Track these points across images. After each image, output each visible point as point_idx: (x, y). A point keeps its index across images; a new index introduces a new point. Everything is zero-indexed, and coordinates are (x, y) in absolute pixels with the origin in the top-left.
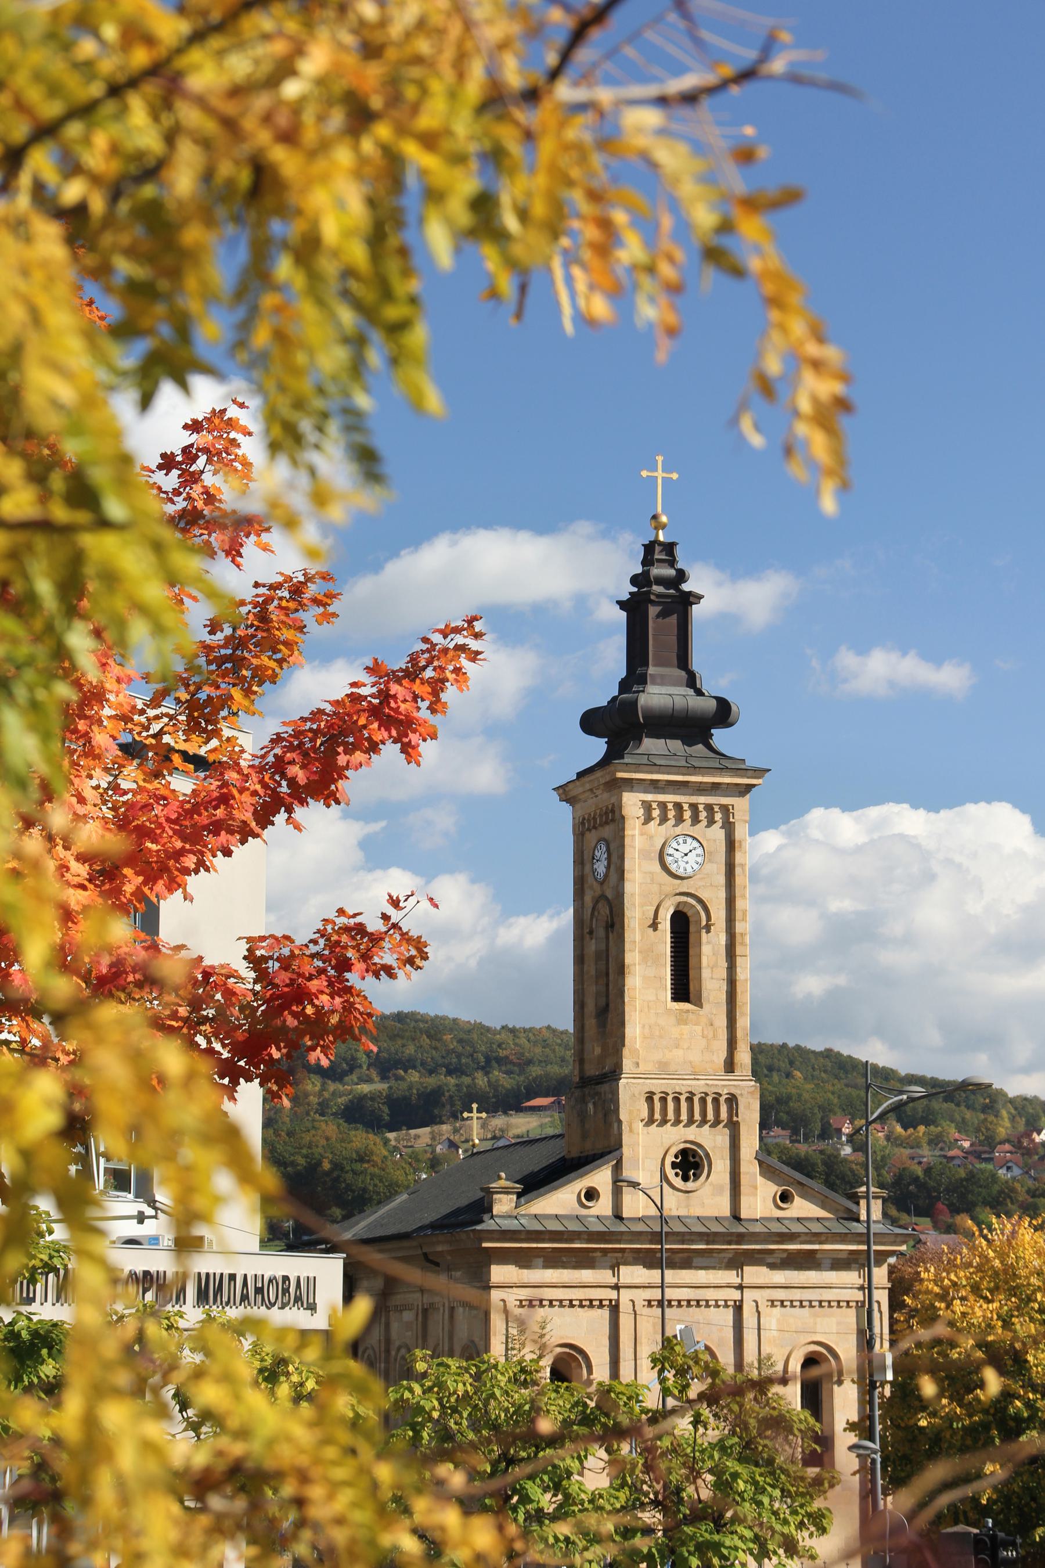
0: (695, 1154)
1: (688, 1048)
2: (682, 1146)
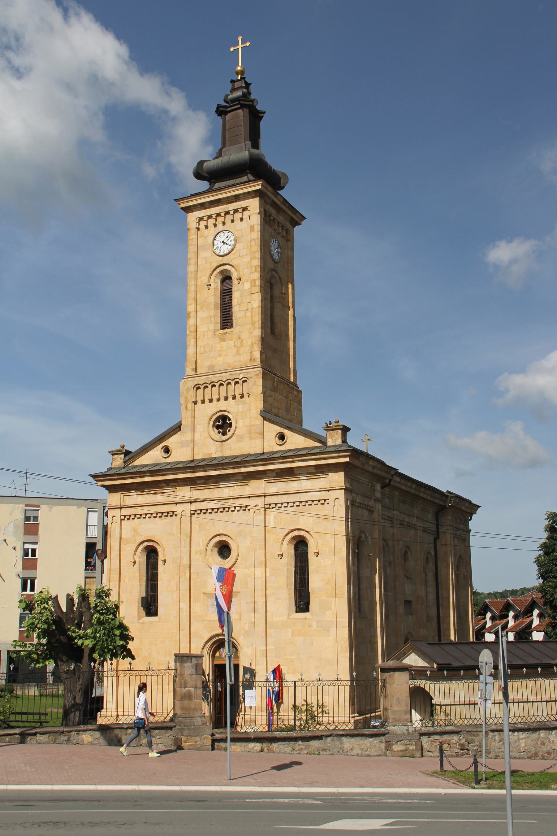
1: (226, 355)
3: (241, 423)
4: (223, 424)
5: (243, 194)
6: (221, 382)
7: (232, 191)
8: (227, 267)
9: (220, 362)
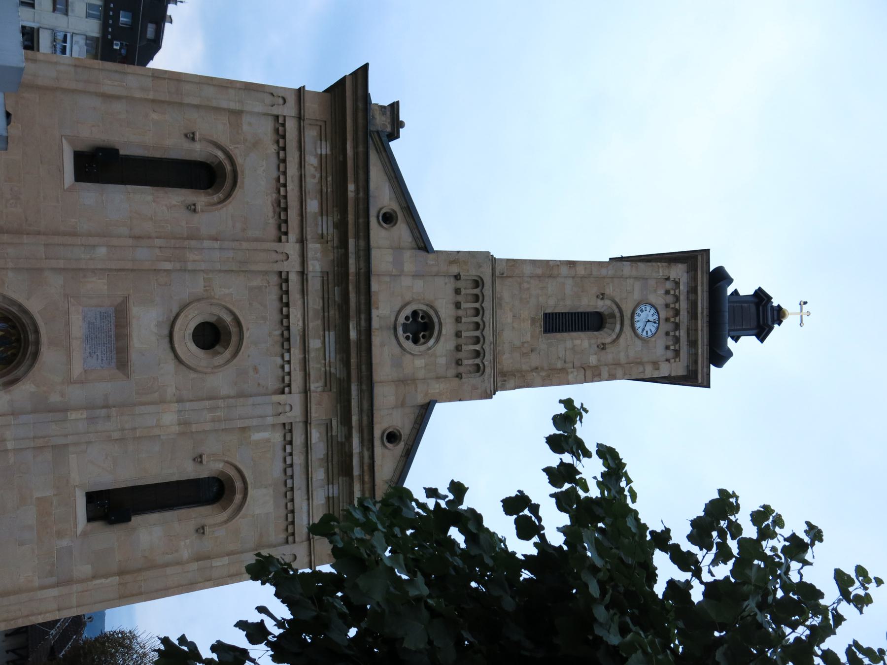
0: (427, 338)
2: (435, 320)
3: (419, 362)
4: (420, 327)
5: (696, 354)
6: (481, 327)
7: (702, 340)
8: (618, 327)
9: (506, 317)
